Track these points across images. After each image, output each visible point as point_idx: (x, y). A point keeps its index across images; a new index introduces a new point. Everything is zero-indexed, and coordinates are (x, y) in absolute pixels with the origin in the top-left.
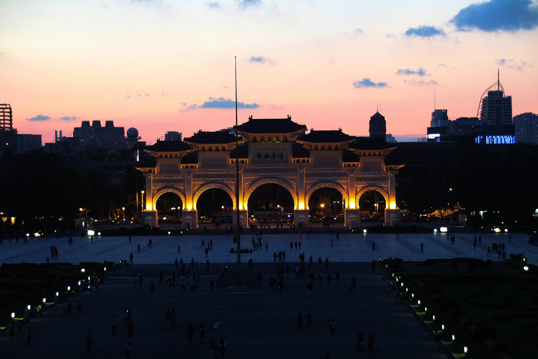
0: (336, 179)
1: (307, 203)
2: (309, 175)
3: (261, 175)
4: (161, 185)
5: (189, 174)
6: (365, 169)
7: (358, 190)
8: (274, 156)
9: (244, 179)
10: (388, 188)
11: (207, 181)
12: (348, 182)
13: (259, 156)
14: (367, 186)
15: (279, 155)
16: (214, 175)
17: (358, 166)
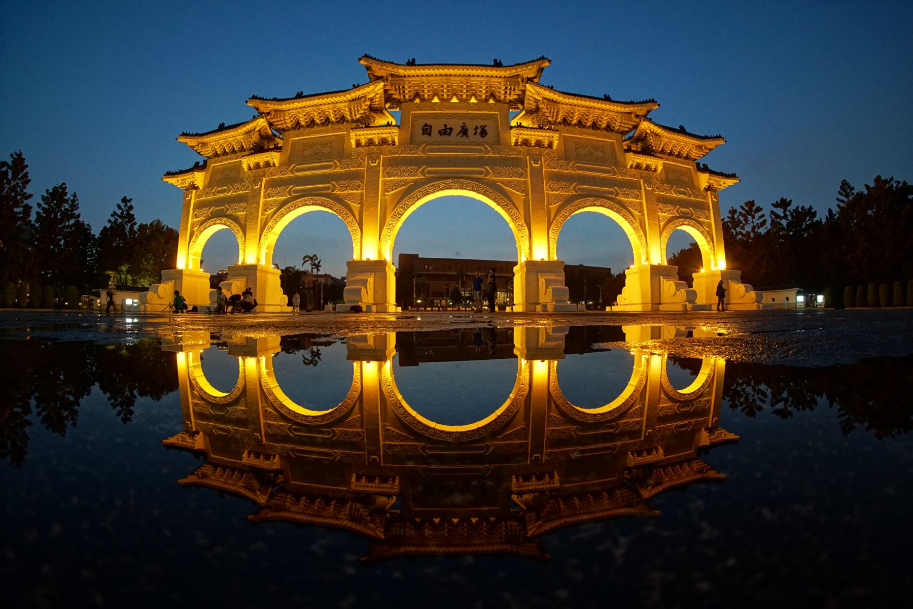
0: (617, 194)
1: (554, 246)
2: (556, 178)
3: (429, 172)
4: (209, 211)
5: (257, 180)
6: (673, 178)
7: (662, 224)
8: (464, 131)
9: (385, 183)
10: (709, 225)
11: (295, 192)
12: (641, 204)
13: (427, 130)
14: (677, 218)
15: (476, 128)
16: (313, 176)
17: (655, 170)
